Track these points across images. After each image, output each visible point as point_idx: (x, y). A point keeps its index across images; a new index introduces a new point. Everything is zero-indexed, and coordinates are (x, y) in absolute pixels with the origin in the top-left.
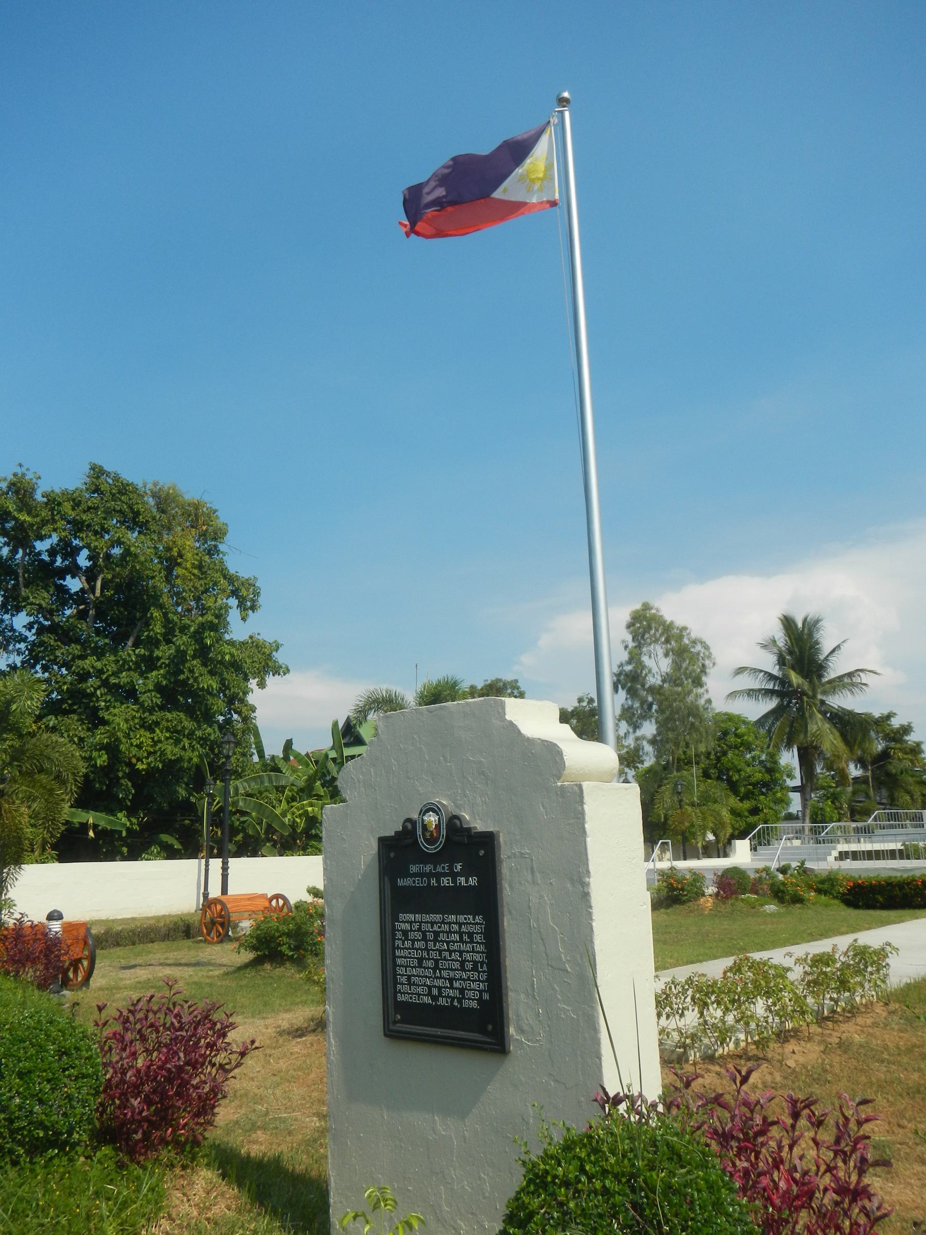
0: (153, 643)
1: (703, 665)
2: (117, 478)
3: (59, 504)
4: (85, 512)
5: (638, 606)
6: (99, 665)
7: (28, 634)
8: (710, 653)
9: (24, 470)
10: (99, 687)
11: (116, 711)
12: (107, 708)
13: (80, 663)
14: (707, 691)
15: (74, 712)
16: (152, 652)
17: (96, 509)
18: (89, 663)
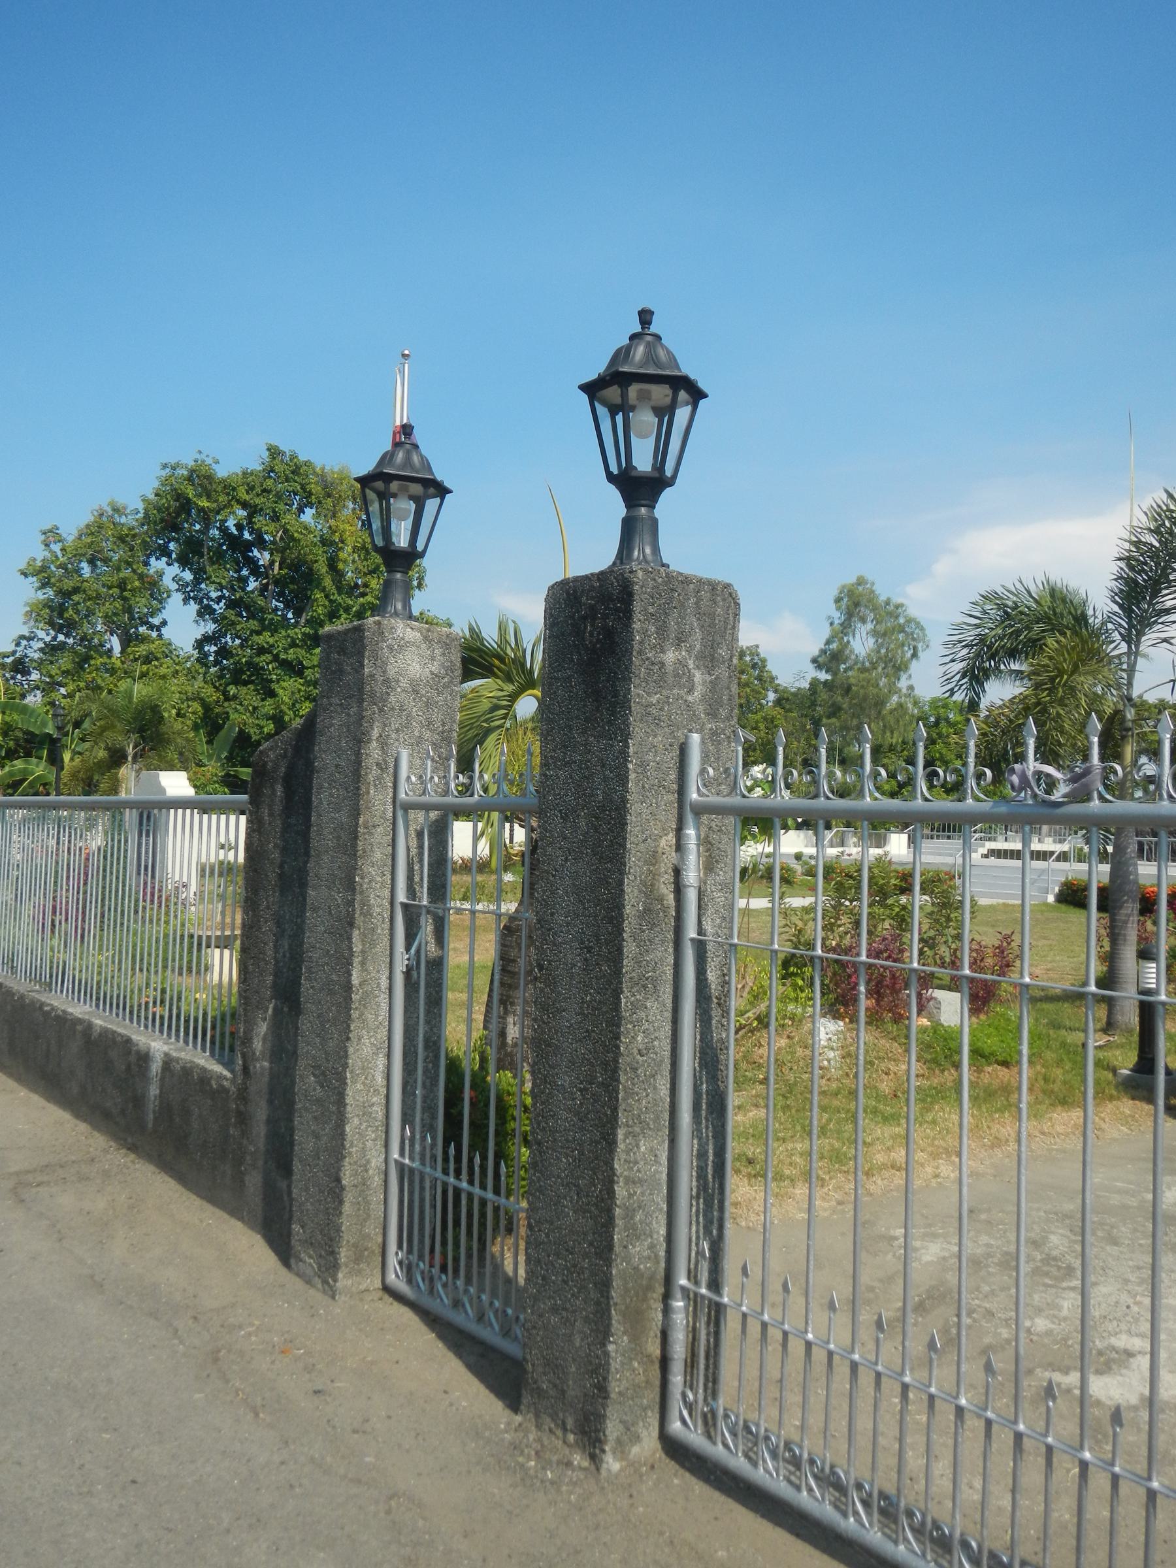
0: (316, 623)
1: (915, 648)
2: (293, 457)
3: (234, 489)
4: (258, 495)
5: (851, 579)
6: (271, 641)
7: (216, 606)
8: (925, 635)
9: (203, 457)
10: (271, 662)
11: (284, 684)
12: (278, 681)
13: (255, 638)
14: (910, 676)
15: (252, 682)
16: (316, 631)
17: (269, 492)
18: (265, 638)
